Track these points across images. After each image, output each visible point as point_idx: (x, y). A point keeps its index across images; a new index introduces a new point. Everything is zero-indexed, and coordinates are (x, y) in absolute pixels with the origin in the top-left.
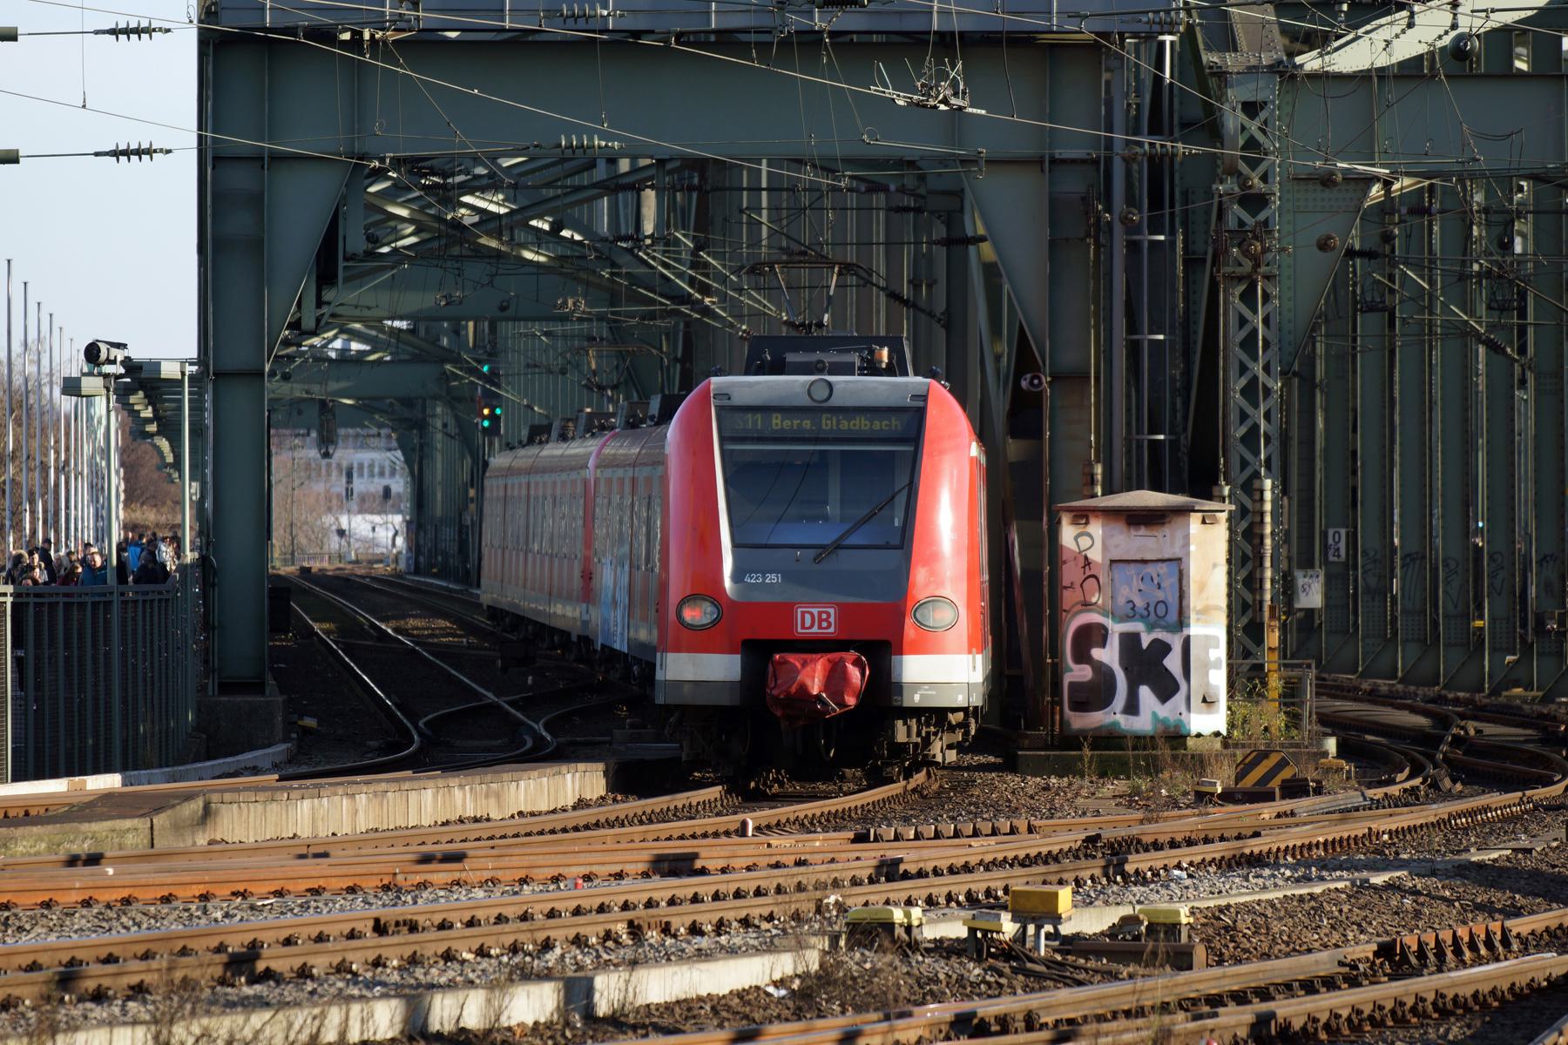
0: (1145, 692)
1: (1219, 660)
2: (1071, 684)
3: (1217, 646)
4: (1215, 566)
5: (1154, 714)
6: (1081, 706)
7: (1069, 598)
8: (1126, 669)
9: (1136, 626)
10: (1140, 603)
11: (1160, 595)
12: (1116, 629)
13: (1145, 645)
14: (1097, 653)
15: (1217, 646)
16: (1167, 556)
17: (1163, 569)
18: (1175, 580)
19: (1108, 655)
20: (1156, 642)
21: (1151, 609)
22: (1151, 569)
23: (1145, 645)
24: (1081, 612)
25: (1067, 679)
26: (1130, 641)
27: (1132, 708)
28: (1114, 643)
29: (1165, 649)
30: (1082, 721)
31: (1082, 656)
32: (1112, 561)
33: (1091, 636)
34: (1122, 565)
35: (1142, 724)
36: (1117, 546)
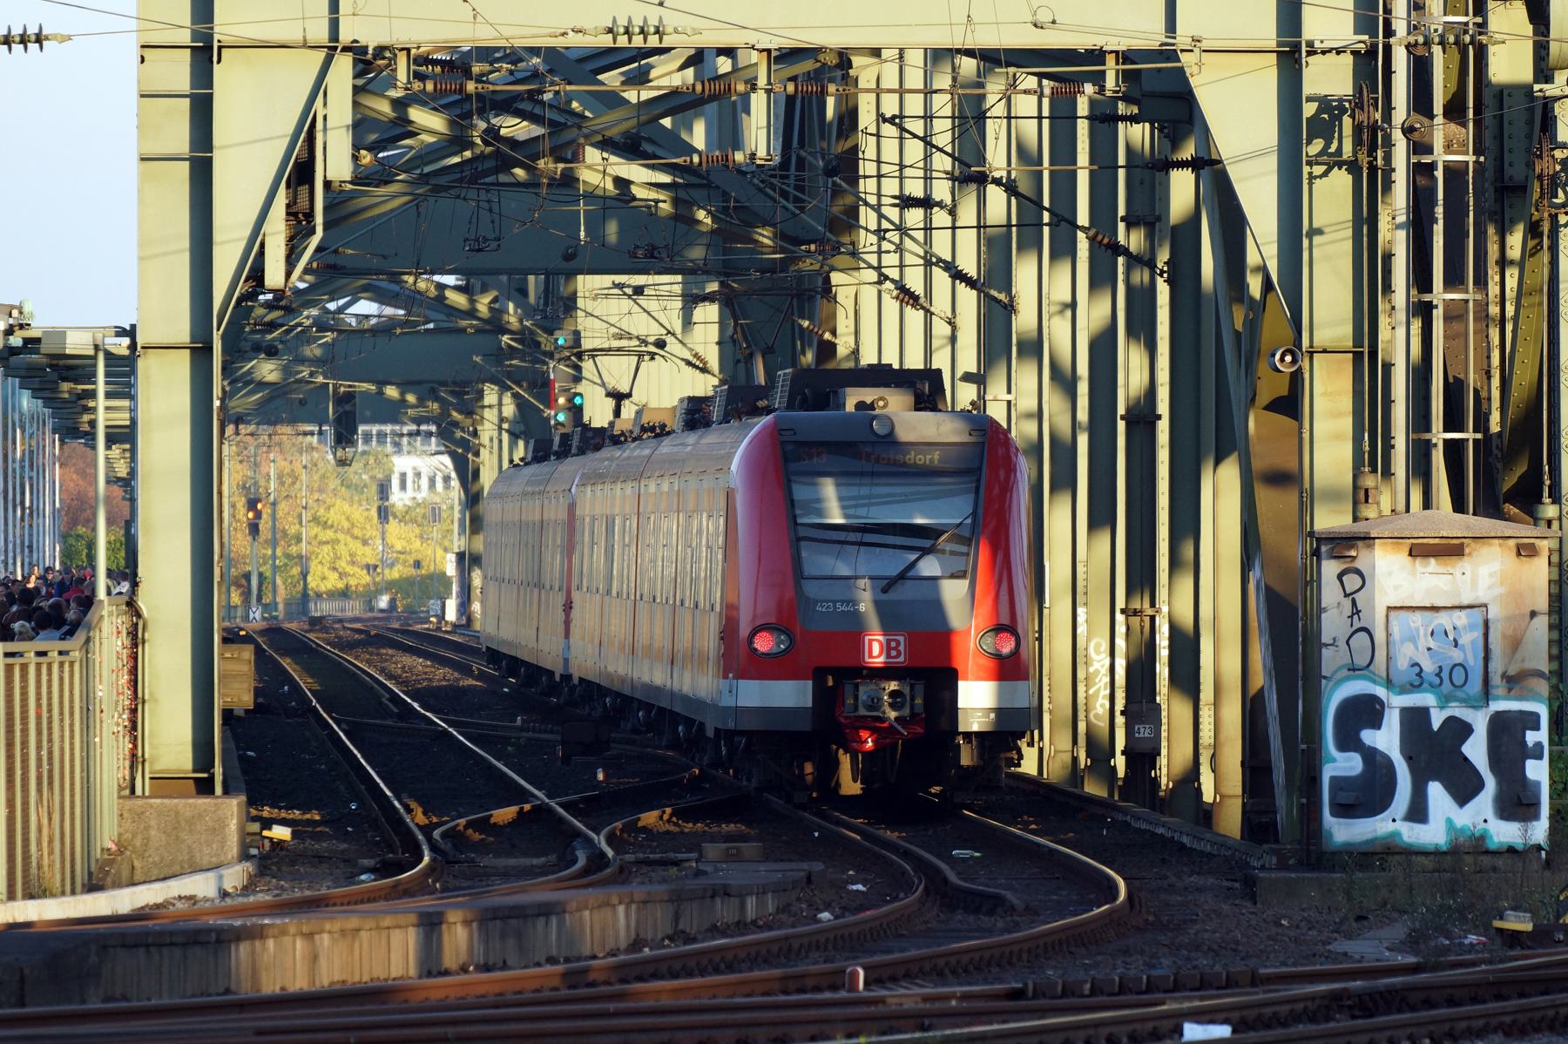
0: (1436, 792)
1: (1539, 745)
2: (1333, 779)
3: (1537, 728)
4: (1533, 614)
5: (1449, 822)
6: (1346, 810)
7: (1330, 660)
8: (1409, 759)
9: (1427, 699)
10: (1429, 667)
11: (1457, 656)
12: (1396, 702)
13: (1436, 725)
14: (1367, 736)
15: (1537, 728)
16: (1466, 602)
17: (1461, 618)
18: (1478, 634)
19: (1386, 738)
20: (1451, 721)
21: (1445, 675)
22: (1444, 620)
23: (1436, 725)
24: (1348, 679)
25: (1328, 772)
26: (1415, 719)
27: (1418, 812)
28: (1392, 721)
29: (1460, 730)
30: (1343, 832)
31: (1348, 741)
32: (1389, 608)
33: (1365, 712)
34: (1403, 614)
35: (1431, 835)
36: (1396, 588)
